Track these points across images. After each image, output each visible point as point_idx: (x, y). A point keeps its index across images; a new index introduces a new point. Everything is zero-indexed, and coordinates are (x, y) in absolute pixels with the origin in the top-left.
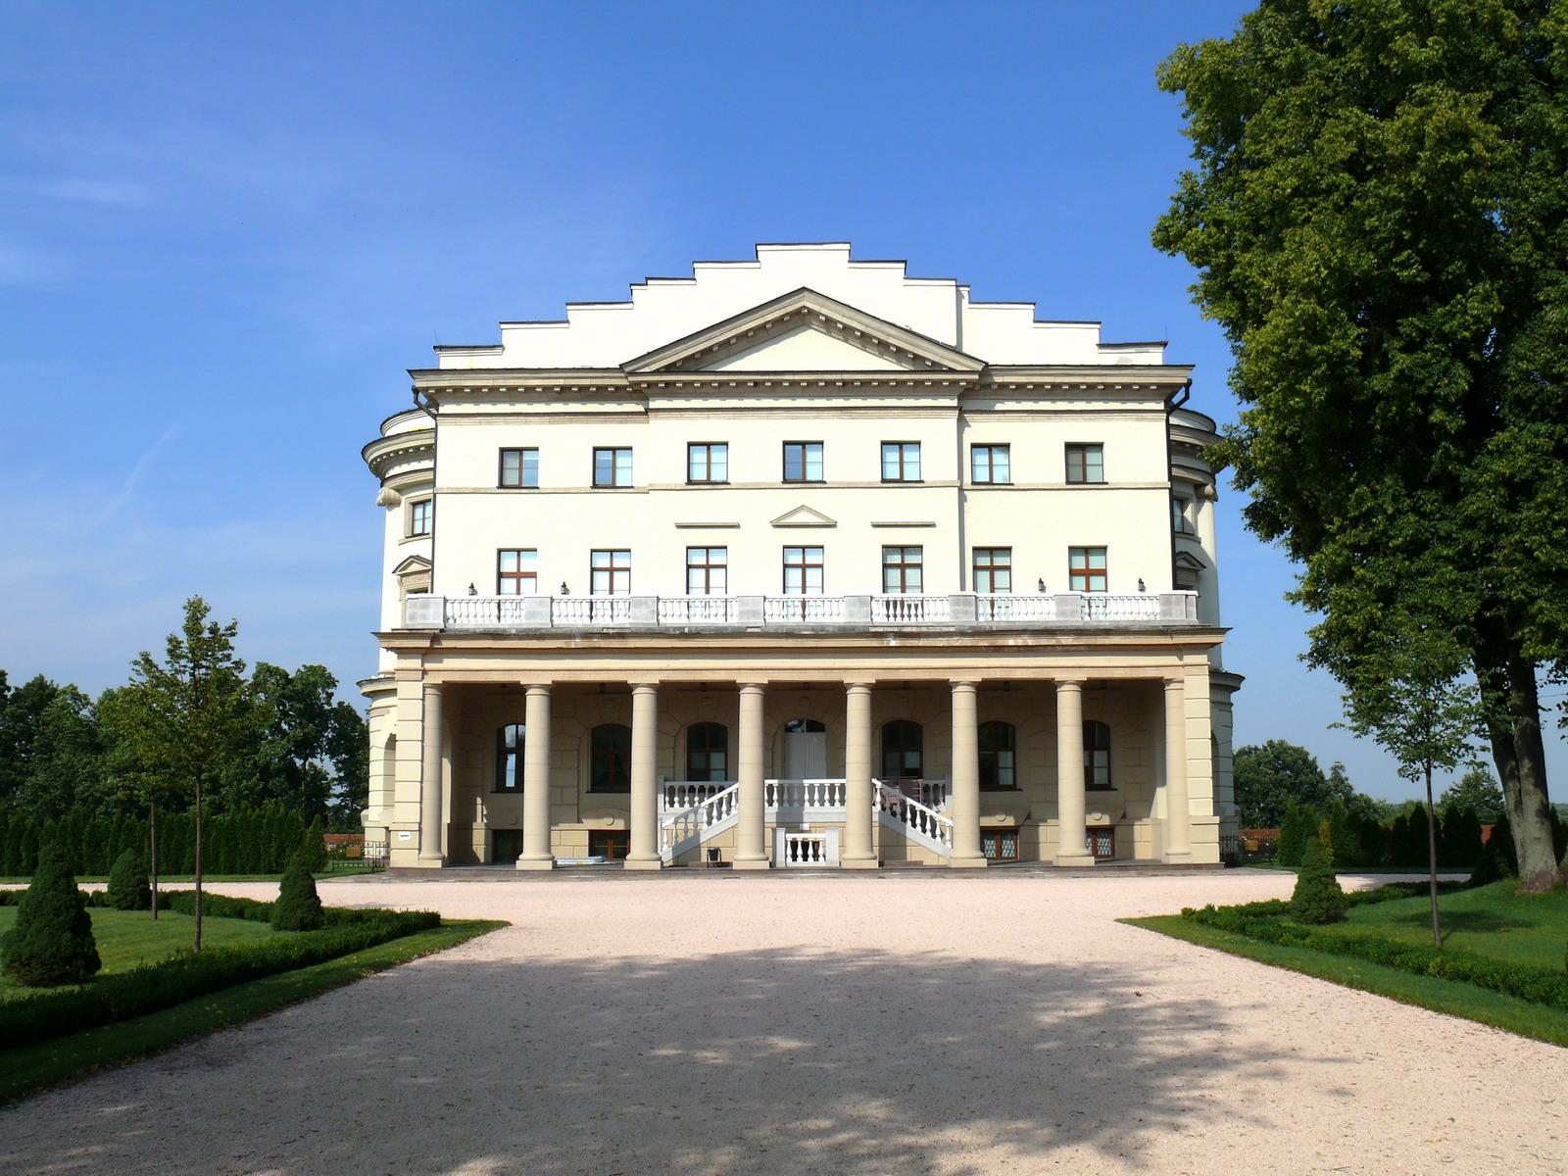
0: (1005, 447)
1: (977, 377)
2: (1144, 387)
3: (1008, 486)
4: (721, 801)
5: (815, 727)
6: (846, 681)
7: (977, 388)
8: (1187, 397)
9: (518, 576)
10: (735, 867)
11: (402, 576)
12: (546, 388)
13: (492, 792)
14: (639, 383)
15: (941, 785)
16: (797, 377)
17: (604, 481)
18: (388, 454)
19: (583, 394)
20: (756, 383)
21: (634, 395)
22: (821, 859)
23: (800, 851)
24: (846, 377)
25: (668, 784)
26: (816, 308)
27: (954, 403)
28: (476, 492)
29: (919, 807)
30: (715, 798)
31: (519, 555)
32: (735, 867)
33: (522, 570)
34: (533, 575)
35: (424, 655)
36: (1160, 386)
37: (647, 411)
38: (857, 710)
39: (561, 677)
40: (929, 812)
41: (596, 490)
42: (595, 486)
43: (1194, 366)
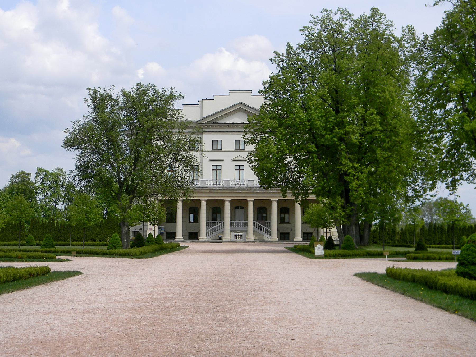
4: (220, 225)
5: (242, 208)
16: (238, 125)
25: (207, 221)
29: (265, 227)
30: (219, 224)
38: (251, 207)
40: (267, 229)
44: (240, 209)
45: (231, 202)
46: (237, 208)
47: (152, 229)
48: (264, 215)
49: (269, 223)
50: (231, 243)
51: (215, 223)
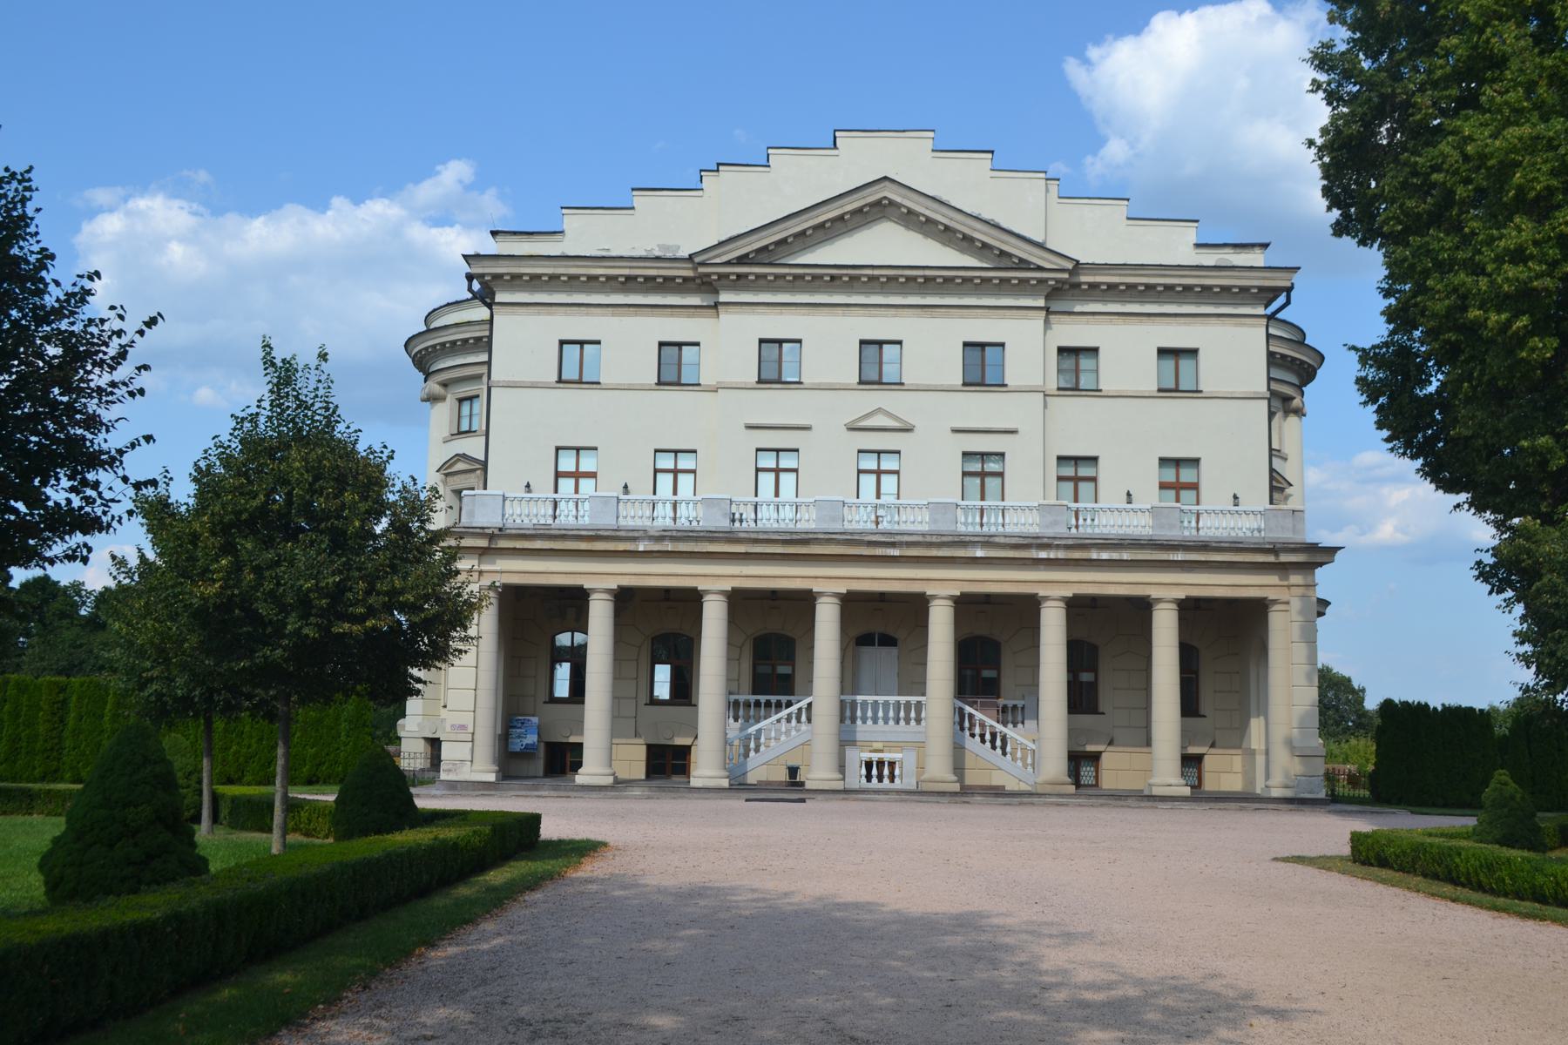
0: (1193, 352)
1: (1066, 276)
2: (1244, 290)
3: (1096, 392)
5: (888, 641)
6: (1042, 593)
7: (1067, 287)
8: (1288, 302)
9: (577, 475)
10: (808, 785)
11: (447, 475)
12: (609, 278)
13: (545, 702)
14: (708, 275)
15: (1020, 706)
16: (876, 272)
17: (770, 378)
18: (434, 346)
19: (649, 285)
20: (833, 278)
21: (703, 287)
22: (897, 780)
23: (875, 772)
24: (928, 273)
26: (898, 199)
27: (1041, 303)
28: (533, 386)
29: (999, 727)
30: (784, 713)
31: (676, 456)
32: (808, 785)
33: (581, 470)
34: (593, 475)
35: (480, 555)
36: (1262, 289)
37: (716, 305)
39: (626, 582)
41: (662, 387)
42: (659, 383)
43: (1299, 268)
44: (882, 644)
45: (851, 603)
46: (865, 640)
47: (463, 727)
48: (986, 673)
49: (1015, 707)
50: (851, 805)
51: (768, 704)
